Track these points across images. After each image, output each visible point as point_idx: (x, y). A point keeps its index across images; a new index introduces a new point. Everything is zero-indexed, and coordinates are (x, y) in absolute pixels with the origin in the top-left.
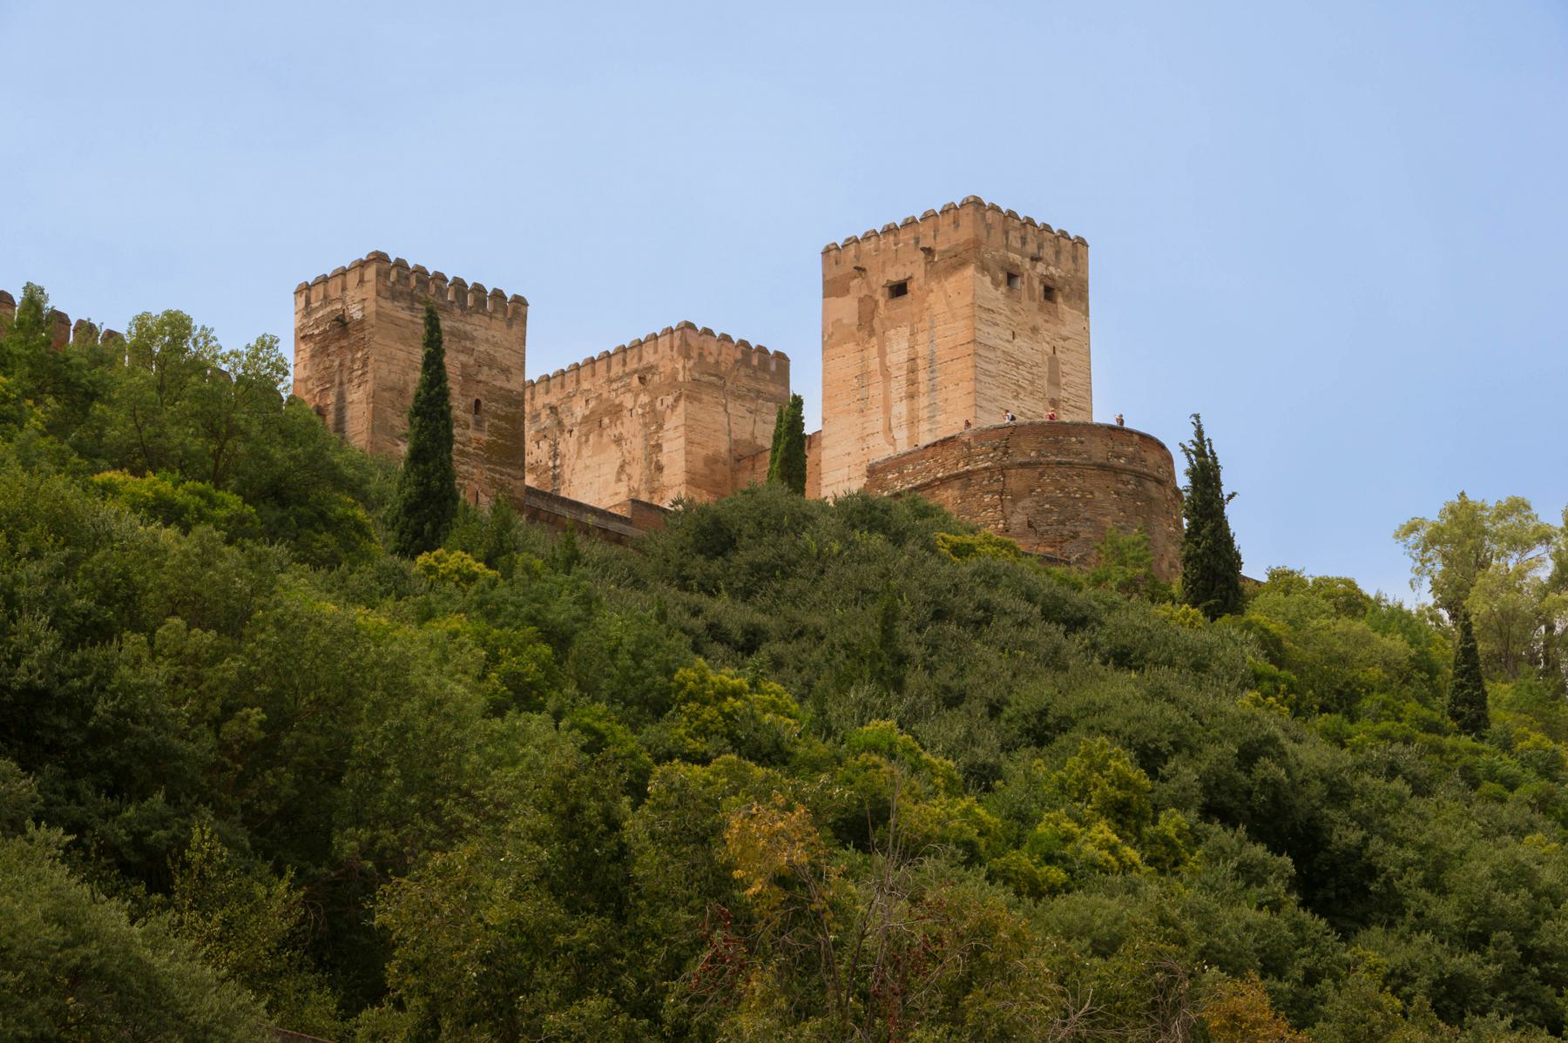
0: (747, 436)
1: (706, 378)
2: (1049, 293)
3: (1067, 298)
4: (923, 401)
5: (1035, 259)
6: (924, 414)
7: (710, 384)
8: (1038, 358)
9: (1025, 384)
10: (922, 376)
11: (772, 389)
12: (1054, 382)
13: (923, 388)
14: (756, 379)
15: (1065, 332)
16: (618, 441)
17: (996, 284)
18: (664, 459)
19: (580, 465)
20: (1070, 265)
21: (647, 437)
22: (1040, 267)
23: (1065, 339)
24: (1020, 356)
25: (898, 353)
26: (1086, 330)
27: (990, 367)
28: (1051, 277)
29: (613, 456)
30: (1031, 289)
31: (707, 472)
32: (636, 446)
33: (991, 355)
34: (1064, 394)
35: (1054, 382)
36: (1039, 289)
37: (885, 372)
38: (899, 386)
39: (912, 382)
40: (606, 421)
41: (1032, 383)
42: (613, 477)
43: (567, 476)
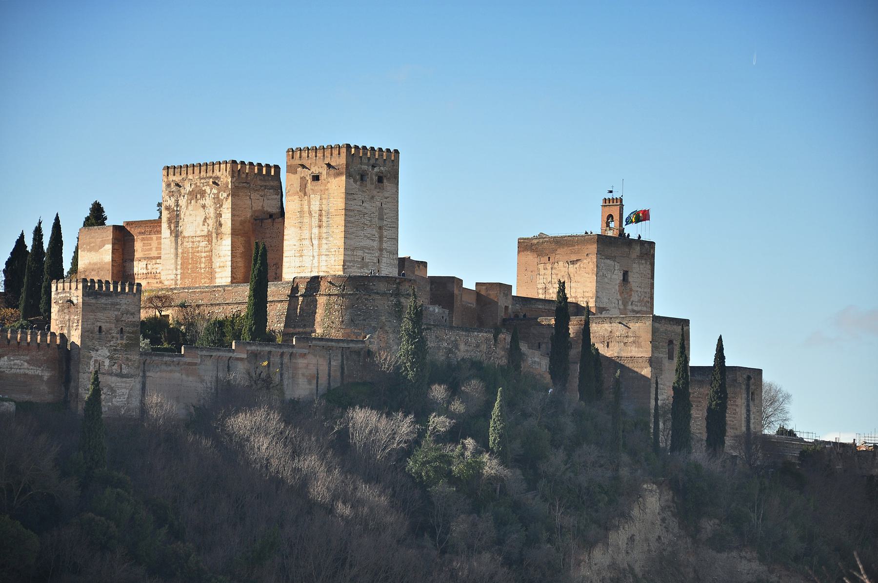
0: (260, 208)
1: (241, 185)
2: (380, 180)
3: (388, 179)
4: (324, 230)
5: (373, 166)
6: (324, 235)
7: (244, 187)
8: (374, 210)
9: (367, 222)
10: (324, 219)
11: (272, 183)
12: (381, 219)
13: (324, 224)
14: (264, 180)
15: (387, 195)
16: (204, 206)
17: (355, 181)
18: (223, 222)
19: (188, 213)
20: (391, 164)
21: (216, 209)
22: (376, 169)
25: (315, 207)
27: (352, 219)
29: (201, 214)
30: (372, 179)
31: (241, 227)
32: (211, 211)
33: (352, 213)
34: (385, 223)
35: (381, 219)
36: (375, 178)
37: (310, 213)
38: (315, 221)
39: (320, 221)
40: (199, 196)
41: (370, 221)
42: (201, 223)
43: (182, 216)
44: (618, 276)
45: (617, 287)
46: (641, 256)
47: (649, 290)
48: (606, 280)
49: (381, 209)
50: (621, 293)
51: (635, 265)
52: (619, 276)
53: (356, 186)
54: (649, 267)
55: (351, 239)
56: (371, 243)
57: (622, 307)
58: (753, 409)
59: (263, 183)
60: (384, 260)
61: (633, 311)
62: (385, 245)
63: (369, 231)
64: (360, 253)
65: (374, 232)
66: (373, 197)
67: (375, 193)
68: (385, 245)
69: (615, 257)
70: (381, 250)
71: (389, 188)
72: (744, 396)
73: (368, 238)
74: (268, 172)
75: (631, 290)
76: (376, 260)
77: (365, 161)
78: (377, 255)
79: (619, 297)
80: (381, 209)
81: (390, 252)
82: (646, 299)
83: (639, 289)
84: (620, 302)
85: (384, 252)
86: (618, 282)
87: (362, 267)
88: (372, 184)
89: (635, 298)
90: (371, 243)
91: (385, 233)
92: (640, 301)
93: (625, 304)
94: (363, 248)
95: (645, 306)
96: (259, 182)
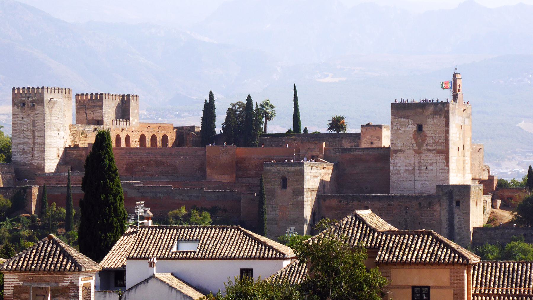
0: (91, 118)
3: (38, 104)
5: (28, 98)
7: (82, 108)
8: (29, 122)
12: (34, 126)
14: (94, 103)
15: (37, 112)
17: (18, 107)
22: (30, 99)
23: (37, 114)
24: (24, 123)
26: (44, 110)
27: (16, 128)
28: (34, 100)
30: (28, 105)
33: (16, 125)
35: (34, 126)
41: (27, 128)
44: (412, 128)
45: (411, 136)
46: (435, 113)
47: (444, 135)
48: (400, 132)
49: (34, 121)
50: (415, 139)
51: (428, 120)
53: (18, 110)
55: (16, 139)
56: (26, 140)
57: (416, 148)
58: (456, 211)
59: (93, 104)
60: (36, 149)
61: (428, 150)
62: (36, 141)
63: (26, 134)
64: (21, 146)
65: (30, 134)
66: (28, 115)
67: (30, 112)
68: (36, 141)
70: (34, 143)
71: (38, 109)
72: (445, 204)
73: (26, 138)
74: (96, 98)
75: (426, 136)
76: (31, 149)
77: (23, 95)
78: (31, 146)
79: (413, 142)
80: (34, 121)
81: (40, 144)
82: (441, 141)
83: (435, 135)
84: (415, 145)
85: (36, 144)
86: (413, 132)
87: (22, 154)
88: (28, 107)
89: (430, 141)
90: (26, 140)
91: (36, 134)
92: (435, 143)
93: (420, 145)
94: (23, 144)
95: (440, 145)
96: (91, 104)
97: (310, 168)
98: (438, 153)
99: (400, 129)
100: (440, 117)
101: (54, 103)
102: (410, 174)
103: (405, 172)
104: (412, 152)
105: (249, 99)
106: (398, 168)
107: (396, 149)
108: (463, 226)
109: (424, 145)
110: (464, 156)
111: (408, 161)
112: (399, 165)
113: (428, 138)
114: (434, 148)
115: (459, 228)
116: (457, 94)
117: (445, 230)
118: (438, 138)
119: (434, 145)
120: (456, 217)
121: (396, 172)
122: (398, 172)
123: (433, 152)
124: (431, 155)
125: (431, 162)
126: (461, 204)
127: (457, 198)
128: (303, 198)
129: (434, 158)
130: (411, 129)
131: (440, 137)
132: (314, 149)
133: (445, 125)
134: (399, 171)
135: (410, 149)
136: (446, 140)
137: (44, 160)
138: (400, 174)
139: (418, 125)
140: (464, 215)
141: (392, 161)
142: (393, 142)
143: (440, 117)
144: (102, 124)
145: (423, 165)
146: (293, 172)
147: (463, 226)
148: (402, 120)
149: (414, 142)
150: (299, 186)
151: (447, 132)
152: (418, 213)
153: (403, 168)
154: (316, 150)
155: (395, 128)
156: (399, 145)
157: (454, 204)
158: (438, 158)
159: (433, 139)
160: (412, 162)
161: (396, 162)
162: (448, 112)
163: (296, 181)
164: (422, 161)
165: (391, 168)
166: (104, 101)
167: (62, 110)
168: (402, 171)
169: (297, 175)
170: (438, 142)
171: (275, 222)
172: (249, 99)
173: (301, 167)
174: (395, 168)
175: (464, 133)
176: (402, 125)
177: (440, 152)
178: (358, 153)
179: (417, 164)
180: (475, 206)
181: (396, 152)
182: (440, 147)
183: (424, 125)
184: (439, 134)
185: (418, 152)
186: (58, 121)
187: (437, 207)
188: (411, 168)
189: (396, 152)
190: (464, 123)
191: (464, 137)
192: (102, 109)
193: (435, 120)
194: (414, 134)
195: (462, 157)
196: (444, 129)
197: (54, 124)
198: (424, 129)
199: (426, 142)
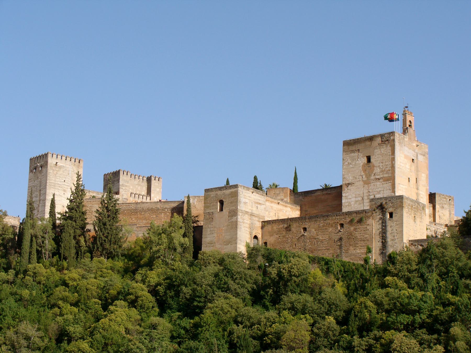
12: (40, 186)
47: (390, 163)
48: (351, 166)
50: (365, 171)
51: (376, 151)
52: (365, 160)
54: (389, 148)
57: (365, 179)
58: (389, 223)
61: (376, 179)
69: (359, 150)
75: (374, 166)
80: (41, 182)
83: (381, 164)
84: (364, 176)
86: (362, 164)
89: (377, 170)
92: (382, 171)
93: (368, 176)
97: (251, 193)
98: (384, 181)
99: (351, 164)
100: (386, 147)
101: (60, 167)
102: (360, 204)
103: (355, 204)
104: (361, 183)
105: (255, 178)
106: (349, 200)
107: (347, 182)
108: (396, 237)
109: (373, 175)
110: (417, 189)
111: (358, 193)
112: (350, 197)
113: (375, 168)
114: (382, 176)
115: (393, 240)
116: (407, 128)
117: (378, 243)
118: (385, 167)
119: (381, 174)
120: (389, 229)
121: (347, 204)
122: (349, 205)
123: (380, 180)
124: (378, 183)
125: (378, 190)
126: (393, 216)
127: (391, 210)
128: (237, 218)
129: (381, 186)
130: (360, 162)
131: (387, 165)
132: (279, 193)
133: (391, 154)
134: (350, 203)
135: (360, 181)
136: (392, 167)
137: (44, 213)
138: (351, 205)
139: (367, 157)
140: (397, 226)
141: (343, 195)
142: (345, 176)
143: (386, 147)
144: (119, 194)
145: (371, 194)
146: (229, 195)
147: (396, 237)
148: (353, 154)
149: (363, 174)
150: (234, 208)
151: (393, 159)
152: (352, 228)
153: (353, 199)
154: (281, 194)
155: (347, 163)
156: (350, 179)
157: (388, 216)
158: (385, 185)
159: (380, 168)
160: (362, 193)
161: (347, 195)
162: (394, 140)
163: (231, 203)
164: (370, 191)
165: (343, 201)
166: (121, 176)
167: (70, 175)
168: (353, 203)
169: (232, 197)
170: (385, 170)
171: (212, 245)
172: (255, 178)
173: (235, 189)
174: (347, 201)
175: (417, 167)
176: (353, 160)
177: (386, 180)
178: (318, 194)
179: (365, 194)
180: (411, 221)
181: (348, 185)
182: (386, 175)
183: (371, 157)
184: (385, 162)
185: (367, 183)
186: (64, 183)
187: (370, 221)
188: (360, 199)
189: (348, 185)
190: (417, 158)
191: (417, 170)
192: (119, 182)
193: (382, 149)
194: (364, 166)
195: (416, 190)
196: (391, 157)
197: (58, 184)
198: (372, 160)
199: (374, 172)
